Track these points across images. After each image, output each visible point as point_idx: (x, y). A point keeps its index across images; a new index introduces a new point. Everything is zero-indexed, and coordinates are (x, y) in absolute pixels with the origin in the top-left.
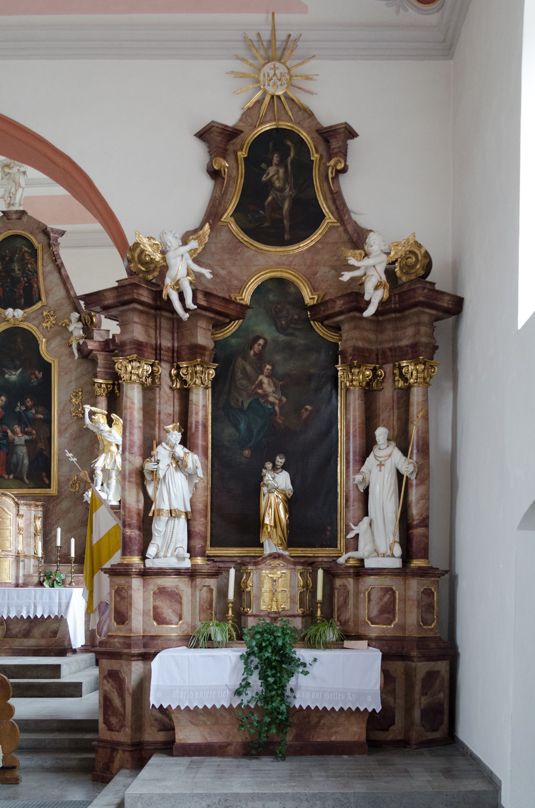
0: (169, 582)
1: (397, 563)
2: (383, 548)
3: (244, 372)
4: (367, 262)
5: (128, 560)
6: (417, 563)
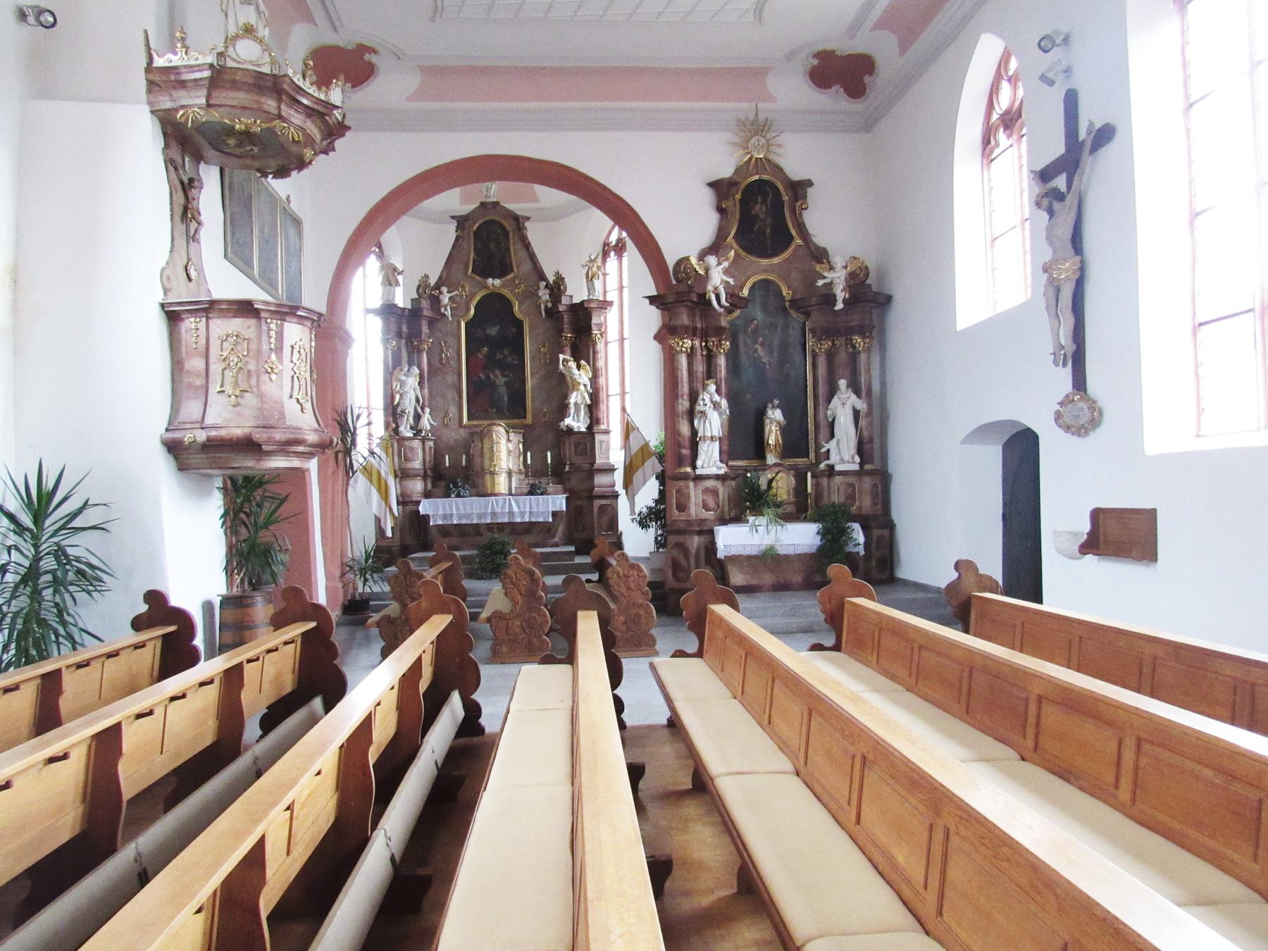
0: (710, 484)
1: (857, 467)
2: (847, 457)
3: (745, 342)
4: (835, 275)
5: (682, 470)
6: (867, 467)
